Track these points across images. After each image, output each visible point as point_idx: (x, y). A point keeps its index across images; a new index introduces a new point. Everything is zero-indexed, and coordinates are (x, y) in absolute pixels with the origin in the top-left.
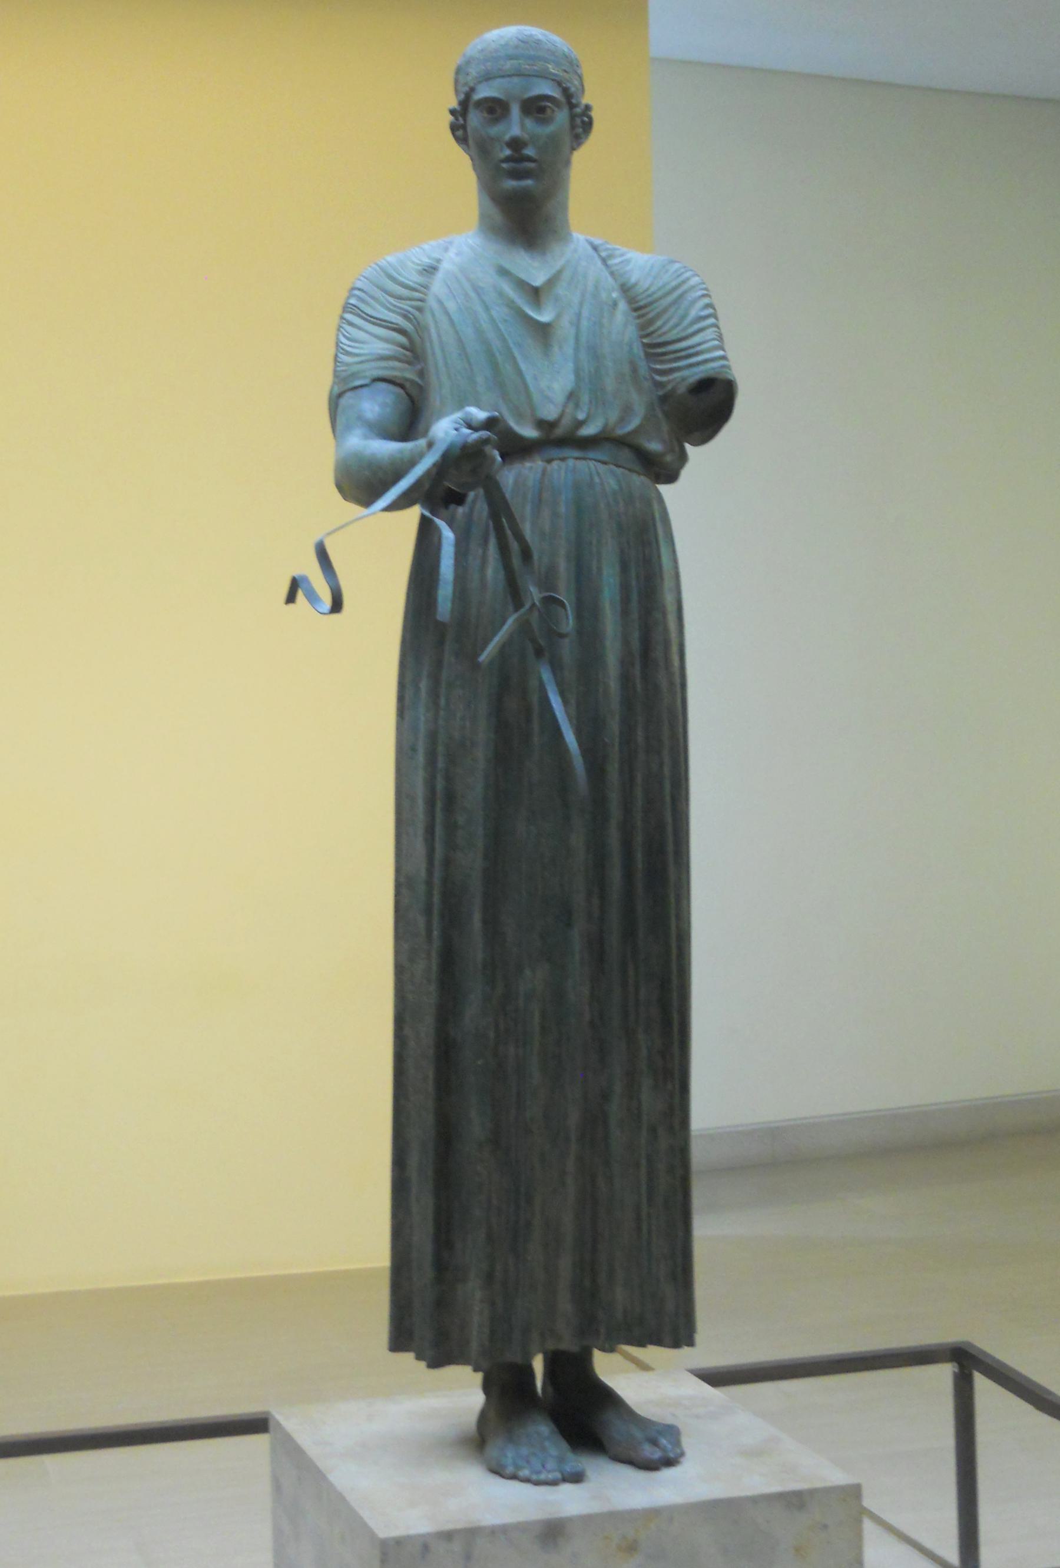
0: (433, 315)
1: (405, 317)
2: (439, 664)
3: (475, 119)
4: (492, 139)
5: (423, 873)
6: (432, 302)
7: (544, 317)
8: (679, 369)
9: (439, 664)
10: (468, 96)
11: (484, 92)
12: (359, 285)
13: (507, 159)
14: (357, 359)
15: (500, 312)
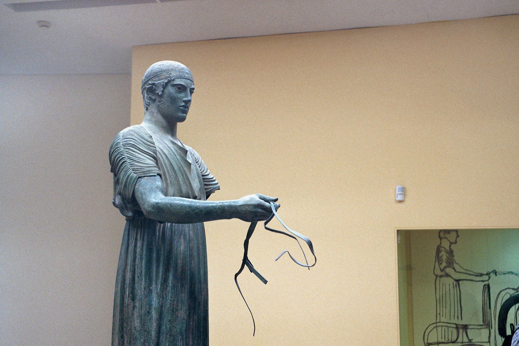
0: (160, 154)
1: (154, 153)
2: (165, 280)
3: (171, 90)
4: (179, 98)
6: (158, 149)
7: (190, 162)
8: (212, 185)
9: (165, 280)
10: (169, 81)
11: (178, 82)
12: (129, 137)
13: (181, 106)
14: (146, 165)
15: (178, 157)
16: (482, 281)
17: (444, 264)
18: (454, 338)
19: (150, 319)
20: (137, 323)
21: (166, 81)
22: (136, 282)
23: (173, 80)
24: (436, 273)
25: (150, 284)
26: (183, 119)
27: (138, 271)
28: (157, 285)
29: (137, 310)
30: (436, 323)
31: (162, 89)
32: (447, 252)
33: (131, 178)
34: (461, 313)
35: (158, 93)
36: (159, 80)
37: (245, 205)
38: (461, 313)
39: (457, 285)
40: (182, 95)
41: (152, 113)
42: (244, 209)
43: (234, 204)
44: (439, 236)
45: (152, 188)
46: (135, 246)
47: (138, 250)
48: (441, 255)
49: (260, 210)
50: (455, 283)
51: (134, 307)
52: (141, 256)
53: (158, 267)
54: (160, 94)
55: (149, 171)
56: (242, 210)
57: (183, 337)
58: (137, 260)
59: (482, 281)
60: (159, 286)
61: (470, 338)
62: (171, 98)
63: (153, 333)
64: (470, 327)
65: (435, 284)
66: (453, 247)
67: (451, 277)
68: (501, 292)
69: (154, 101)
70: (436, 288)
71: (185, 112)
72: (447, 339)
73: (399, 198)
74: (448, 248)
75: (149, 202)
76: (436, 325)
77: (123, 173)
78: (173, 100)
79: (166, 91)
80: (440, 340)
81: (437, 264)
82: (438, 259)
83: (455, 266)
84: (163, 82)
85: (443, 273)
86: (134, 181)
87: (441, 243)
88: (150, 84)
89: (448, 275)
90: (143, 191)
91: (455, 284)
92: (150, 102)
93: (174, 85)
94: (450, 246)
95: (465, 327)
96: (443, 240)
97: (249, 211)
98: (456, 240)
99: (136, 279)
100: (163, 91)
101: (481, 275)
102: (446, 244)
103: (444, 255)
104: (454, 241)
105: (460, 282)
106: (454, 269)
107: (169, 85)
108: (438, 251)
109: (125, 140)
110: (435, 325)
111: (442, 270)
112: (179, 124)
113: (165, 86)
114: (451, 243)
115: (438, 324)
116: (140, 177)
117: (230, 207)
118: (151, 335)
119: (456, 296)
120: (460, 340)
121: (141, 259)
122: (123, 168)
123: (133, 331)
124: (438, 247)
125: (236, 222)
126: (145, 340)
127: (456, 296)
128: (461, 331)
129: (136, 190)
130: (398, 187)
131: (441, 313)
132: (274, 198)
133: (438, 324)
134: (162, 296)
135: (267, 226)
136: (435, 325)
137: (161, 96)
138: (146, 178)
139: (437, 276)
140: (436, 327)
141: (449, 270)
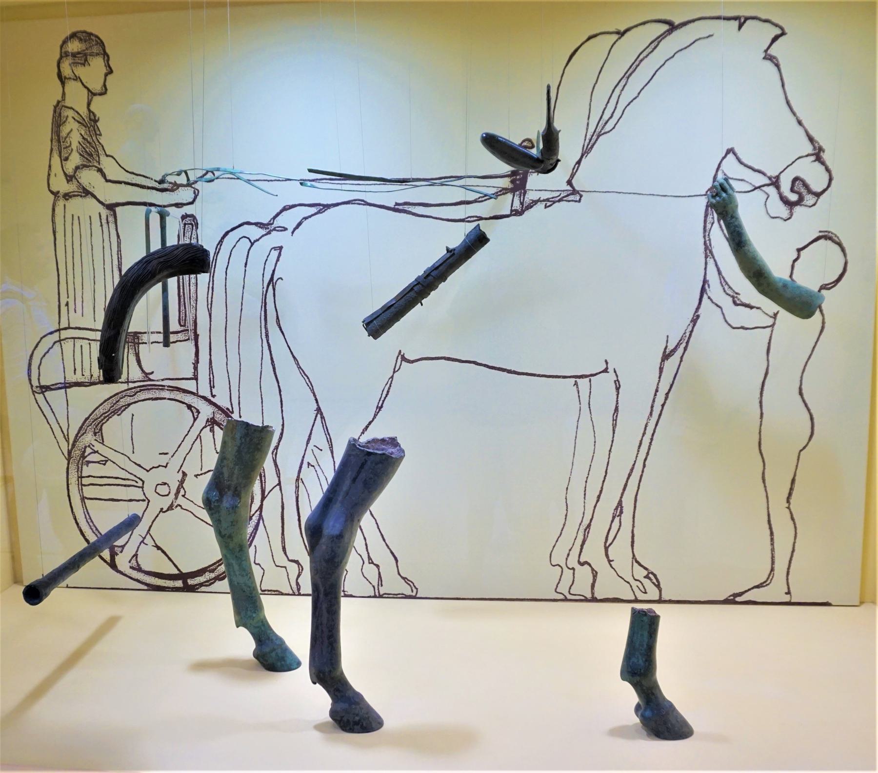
16: (178, 205)
17: (75, 159)
24: (55, 189)
30: (59, 330)
39: (111, 219)
44: (60, 75)
50: (104, 212)
59: (178, 205)
61: (147, 371)
65: (53, 222)
66: (98, 105)
68: (227, 233)
72: (87, 373)
74: (83, 111)
80: (72, 378)
81: (56, 160)
82: (60, 146)
83: (107, 164)
85: (72, 187)
87: (64, 94)
89: (86, 193)
91: (104, 217)
94: (89, 104)
96: (71, 86)
98: (105, 85)
101: (176, 186)
102: (76, 97)
103: (74, 132)
104: (97, 87)
105: (118, 210)
106: (100, 170)
108: (58, 122)
110: (55, 337)
111: (69, 178)
114: (92, 94)
124: (55, 107)
133: (64, 334)
136: (55, 337)
139: (56, 194)
140: (60, 341)
141: (89, 178)
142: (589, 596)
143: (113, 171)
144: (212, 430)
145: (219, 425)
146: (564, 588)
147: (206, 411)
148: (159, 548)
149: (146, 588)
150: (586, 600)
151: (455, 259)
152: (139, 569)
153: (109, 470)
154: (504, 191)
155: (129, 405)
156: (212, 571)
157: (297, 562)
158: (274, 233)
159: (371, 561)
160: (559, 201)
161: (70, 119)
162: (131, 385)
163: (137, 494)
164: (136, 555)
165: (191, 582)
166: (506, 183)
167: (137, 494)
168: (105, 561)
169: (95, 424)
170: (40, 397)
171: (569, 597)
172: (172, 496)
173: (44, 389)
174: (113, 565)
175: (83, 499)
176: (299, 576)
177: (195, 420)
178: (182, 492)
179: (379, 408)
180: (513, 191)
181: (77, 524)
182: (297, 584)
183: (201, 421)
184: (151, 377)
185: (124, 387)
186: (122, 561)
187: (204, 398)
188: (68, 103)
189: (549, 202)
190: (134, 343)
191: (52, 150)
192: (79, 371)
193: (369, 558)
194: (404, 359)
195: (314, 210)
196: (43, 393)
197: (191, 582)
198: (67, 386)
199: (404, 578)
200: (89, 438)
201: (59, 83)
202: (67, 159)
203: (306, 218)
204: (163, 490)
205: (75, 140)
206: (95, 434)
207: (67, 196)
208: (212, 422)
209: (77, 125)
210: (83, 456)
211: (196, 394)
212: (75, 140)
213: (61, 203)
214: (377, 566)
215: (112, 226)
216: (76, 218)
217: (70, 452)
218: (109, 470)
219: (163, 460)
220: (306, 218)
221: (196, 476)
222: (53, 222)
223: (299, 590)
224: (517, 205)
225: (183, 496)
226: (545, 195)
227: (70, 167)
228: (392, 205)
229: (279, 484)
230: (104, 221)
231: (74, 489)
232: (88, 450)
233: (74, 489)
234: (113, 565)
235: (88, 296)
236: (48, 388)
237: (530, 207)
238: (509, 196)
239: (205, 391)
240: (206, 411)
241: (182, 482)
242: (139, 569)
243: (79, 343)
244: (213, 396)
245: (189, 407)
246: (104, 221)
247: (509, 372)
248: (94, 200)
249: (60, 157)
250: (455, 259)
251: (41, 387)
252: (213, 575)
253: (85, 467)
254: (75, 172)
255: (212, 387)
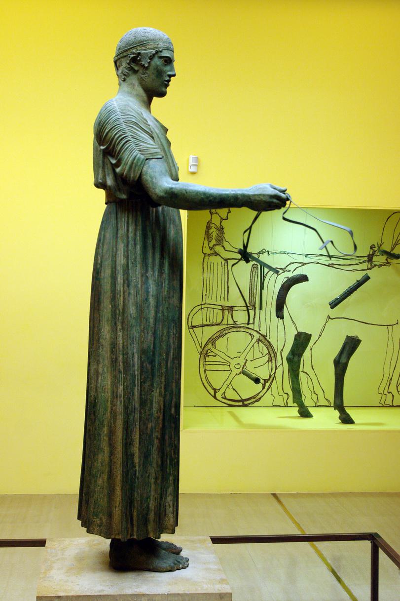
3: (157, 62)
5: (152, 347)
10: (157, 52)
11: (166, 54)
17: (214, 242)
18: (219, 321)
19: (148, 307)
20: (132, 310)
21: (154, 52)
22: (130, 268)
23: (161, 52)
25: (147, 271)
26: (162, 94)
27: (131, 257)
28: (154, 272)
29: (132, 297)
30: (202, 305)
31: (149, 61)
32: (217, 229)
33: (139, 159)
34: (228, 294)
35: (144, 65)
36: (145, 50)
37: (260, 195)
38: (228, 294)
39: (226, 264)
40: (168, 68)
41: (133, 85)
42: (258, 199)
43: (234, 192)
45: (161, 171)
46: (128, 230)
47: (131, 235)
48: (211, 231)
49: (275, 201)
50: (224, 262)
51: (129, 293)
52: (135, 240)
53: (154, 253)
54: (146, 65)
55: (156, 153)
56: (255, 200)
57: (176, 324)
58: (130, 245)
60: (156, 274)
62: (157, 71)
63: (151, 321)
64: (236, 308)
65: (203, 264)
66: (224, 223)
67: (220, 256)
69: (135, 72)
70: (203, 268)
71: (167, 86)
72: (211, 321)
73: (193, 169)
74: (218, 225)
75: (160, 186)
76: (202, 306)
77: (127, 153)
78: (159, 73)
79: (153, 63)
80: (205, 323)
81: (206, 241)
83: (225, 244)
84: (150, 53)
85: (212, 252)
86: (142, 162)
87: (211, 218)
88: (134, 53)
89: (217, 254)
90: (152, 174)
92: (130, 72)
93: (161, 57)
94: (221, 223)
95: (231, 309)
96: (214, 216)
97: (264, 201)
98: (227, 217)
99: (130, 265)
100: (149, 63)
102: (216, 220)
103: (214, 232)
104: (224, 217)
106: (223, 246)
107: (156, 56)
108: (208, 228)
109: (126, 116)
110: (200, 307)
111: (211, 249)
112: (155, 99)
113: (151, 58)
115: (203, 306)
116: (147, 159)
117: (244, 196)
118: (149, 322)
119: (223, 276)
120: (225, 322)
121: (135, 244)
122: (127, 148)
123: (129, 317)
125: (245, 210)
126: (144, 328)
127: (223, 276)
128: (226, 313)
129: (144, 173)
130: (191, 156)
131: (208, 295)
132: (283, 188)
133: (203, 306)
134: (159, 285)
135: (286, 216)
136: (200, 307)
137: (147, 68)
138: (153, 160)
139: (205, 254)
140: (202, 309)
141: (218, 249)
142: (391, 405)
143: (228, 247)
144: (258, 343)
145: (261, 341)
146: (382, 402)
147: (257, 336)
148: (234, 389)
149: (227, 406)
150: (390, 406)
151: (359, 284)
152: (225, 398)
153: (217, 359)
154: (365, 261)
155: (227, 333)
156: (254, 398)
157: (287, 394)
158: (286, 272)
159: (315, 393)
160: (383, 265)
161: (213, 227)
162: (229, 326)
163: (227, 368)
164: (224, 393)
165: (245, 403)
166: (366, 259)
167: (227, 368)
168: (212, 395)
169: (213, 341)
170: (191, 330)
171: (384, 405)
172: (241, 369)
173: (193, 327)
174: (215, 397)
175: (205, 370)
176: (288, 399)
177: (252, 339)
178: (245, 367)
179: (320, 335)
180: (368, 261)
181: (202, 380)
182: (287, 402)
183: (255, 340)
184: (236, 323)
185: (226, 326)
186: (219, 395)
187: (256, 331)
188: (213, 222)
189: (380, 266)
190: (231, 310)
191: (205, 238)
192: (208, 321)
193: (314, 392)
194: (330, 318)
195: (301, 265)
196: (193, 328)
197: (245, 403)
198: (203, 326)
199: (326, 399)
200: (210, 346)
201: (210, 214)
202: (210, 242)
203: (297, 267)
204: (238, 366)
205: (214, 235)
206: (212, 344)
207: (209, 255)
208: (259, 340)
209: (215, 230)
210: (207, 353)
211: (253, 330)
212: (214, 235)
213: (207, 258)
214: (317, 395)
215: (226, 267)
216: (212, 263)
217: (201, 352)
218: (217, 359)
219: (239, 355)
220: (297, 267)
221: (251, 361)
222: (203, 264)
223: (287, 405)
224: (369, 266)
225: (245, 369)
226: (379, 264)
227: (211, 244)
228: (328, 264)
229: (282, 364)
230: (223, 265)
231: (202, 366)
232: (209, 351)
233: (202, 366)
234: (215, 397)
235: (215, 290)
236: (195, 327)
237: (374, 267)
238: (367, 263)
239: (257, 328)
240: (257, 336)
241: (245, 363)
242: (225, 398)
243: (209, 310)
244: (260, 330)
245: (250, 334)
246: (223, 265)
247: (365, 323)
248: (220, 257)
249: (208, 240)
250: (359, 284)
251: (192, 326)
252: (254, 400)
253: (207, 358)
254: (213, 246)
255: (259, 327)
